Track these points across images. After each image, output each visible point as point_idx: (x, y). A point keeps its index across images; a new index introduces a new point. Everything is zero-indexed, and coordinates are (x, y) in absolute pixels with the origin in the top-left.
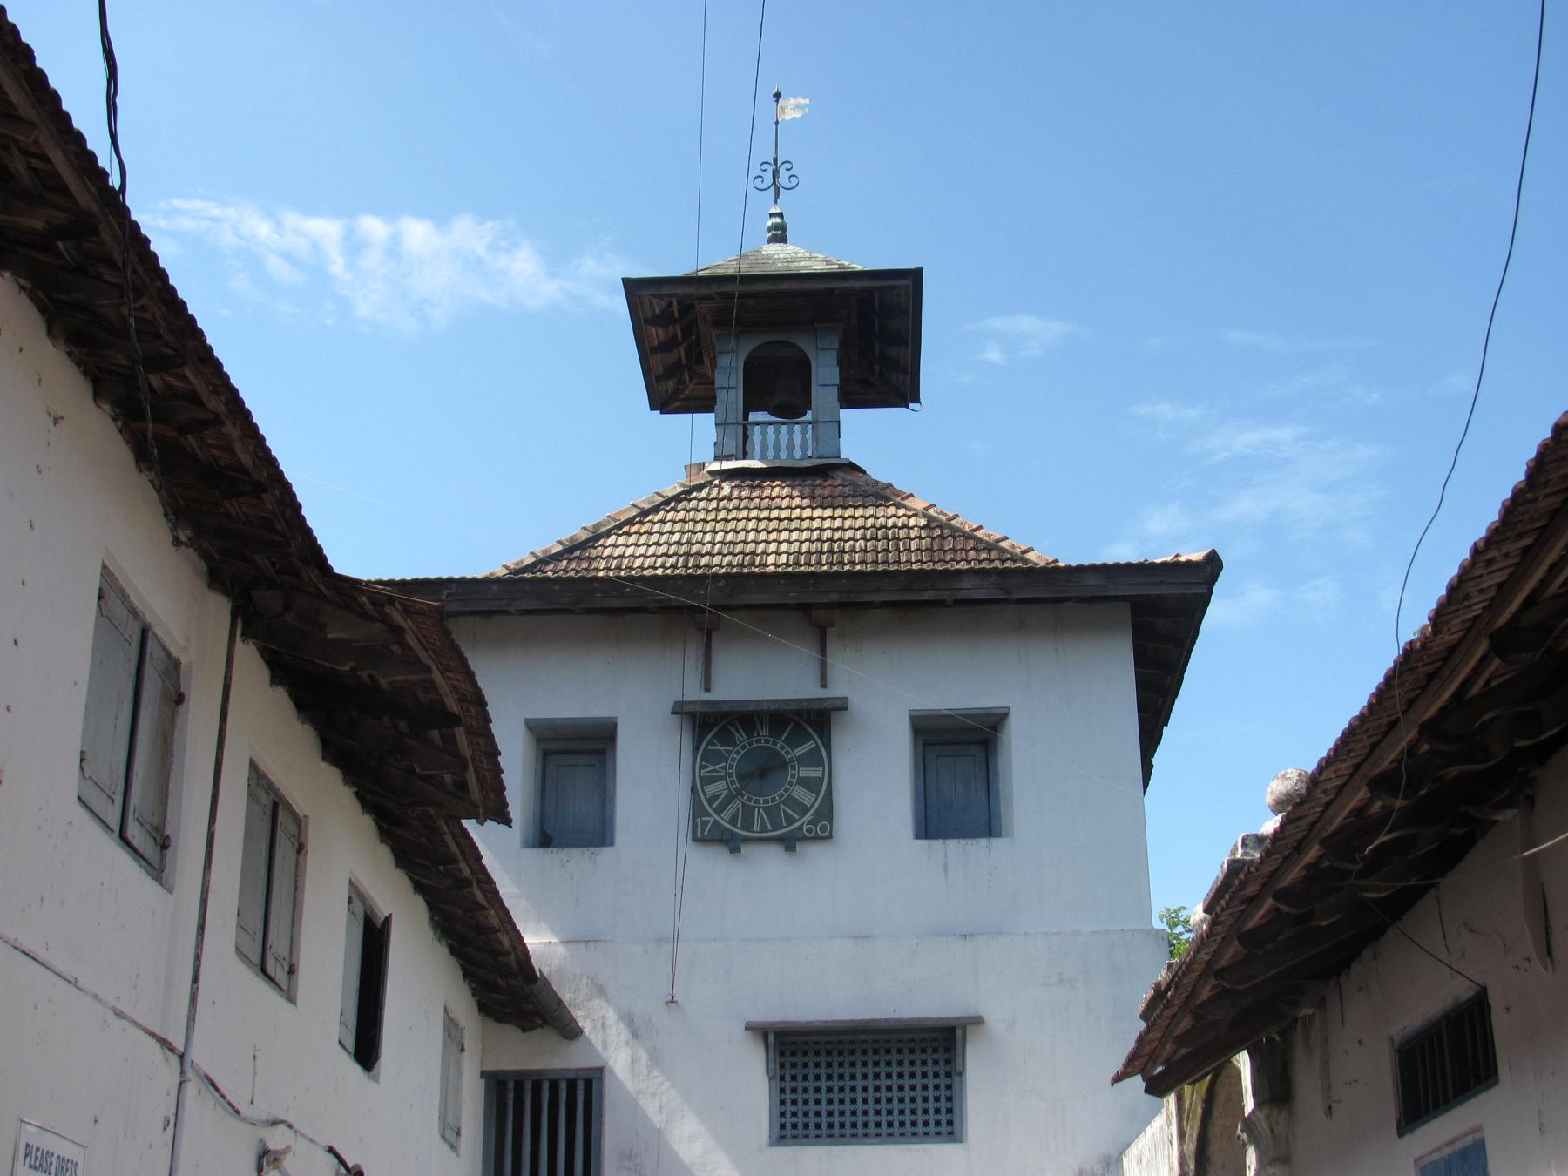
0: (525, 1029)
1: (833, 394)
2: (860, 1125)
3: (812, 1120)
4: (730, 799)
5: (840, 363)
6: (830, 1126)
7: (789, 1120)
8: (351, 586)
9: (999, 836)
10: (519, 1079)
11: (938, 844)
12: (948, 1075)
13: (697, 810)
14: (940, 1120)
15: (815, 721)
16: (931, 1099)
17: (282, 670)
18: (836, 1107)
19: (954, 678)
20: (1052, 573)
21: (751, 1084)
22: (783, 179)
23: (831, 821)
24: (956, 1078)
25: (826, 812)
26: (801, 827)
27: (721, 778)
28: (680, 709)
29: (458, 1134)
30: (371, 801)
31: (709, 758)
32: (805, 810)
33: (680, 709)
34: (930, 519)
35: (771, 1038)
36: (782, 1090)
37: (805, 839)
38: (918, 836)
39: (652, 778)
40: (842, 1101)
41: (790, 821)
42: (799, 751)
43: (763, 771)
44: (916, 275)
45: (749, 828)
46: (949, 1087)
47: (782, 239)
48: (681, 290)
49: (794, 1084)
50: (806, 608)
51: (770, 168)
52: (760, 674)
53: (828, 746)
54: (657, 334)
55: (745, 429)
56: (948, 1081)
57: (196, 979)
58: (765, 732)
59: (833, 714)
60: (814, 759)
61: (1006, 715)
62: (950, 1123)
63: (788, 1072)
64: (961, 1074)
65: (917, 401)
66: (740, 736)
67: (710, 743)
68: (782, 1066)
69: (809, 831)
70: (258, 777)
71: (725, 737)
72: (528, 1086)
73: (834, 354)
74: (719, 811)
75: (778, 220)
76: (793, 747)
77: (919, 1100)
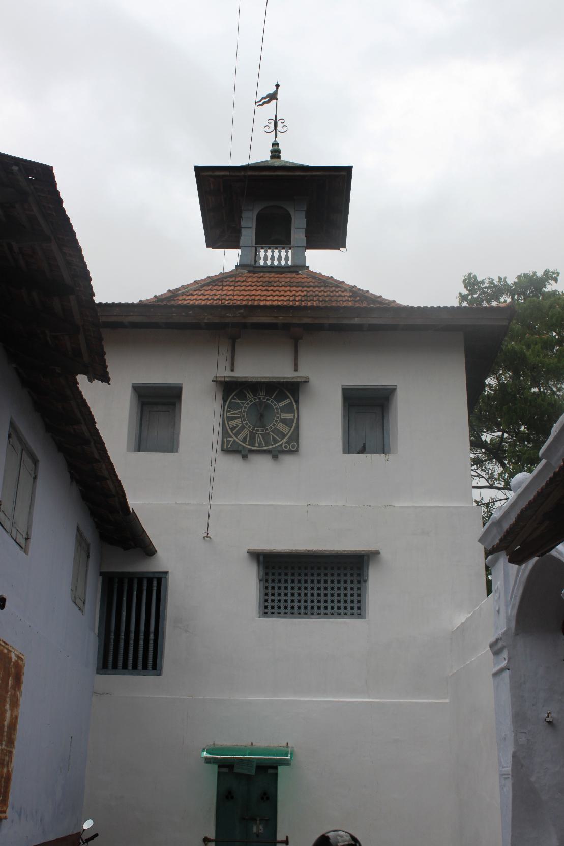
0: (125, 549)
2: (309, 608)
3: (282, 604)
4: (243, 428)
6: (293, 608)
7: (269, 604)
10: (121, 577)
12: (359, 582)
13: (225, 434)
14: (353, 606)
16: (349, 595)
18: (296, 598)
21: (249, 582)
22: (280, 128)
23: (298, 442)
24: (363, 584)
25: (295, 437)
27: (238, 417)
29: (84, 603)
31: (232, 406)
32: (284, 436)
35: (261, 558)
36: (267, 588)
37: (284, 452)
38: (344, 452)
39: (201, 416)
40: (299, 595)
41: (275, 441)
42: (282, 404)
43: (261, 415)
44: (349, 170)
45: (252, 444)
46: (359, 589)
49: (273, 584)
50: (286, 327)
51: (273, 122)
53: (297, 402)
55: (256, 250)
56: (358, 585)
60: (289, 409)
62: (359, 608)
63: (270, 578)
64: (365, 581)
65: (344, 247)
66: (250, 396)
67: (233, 398)
68: (267, 574)
69: (286, 447)
72: (126, 581)
73: (303, 214)
74: (236, 435)
75: (276, 147)
76: (279, 402)
77: (342, 595)
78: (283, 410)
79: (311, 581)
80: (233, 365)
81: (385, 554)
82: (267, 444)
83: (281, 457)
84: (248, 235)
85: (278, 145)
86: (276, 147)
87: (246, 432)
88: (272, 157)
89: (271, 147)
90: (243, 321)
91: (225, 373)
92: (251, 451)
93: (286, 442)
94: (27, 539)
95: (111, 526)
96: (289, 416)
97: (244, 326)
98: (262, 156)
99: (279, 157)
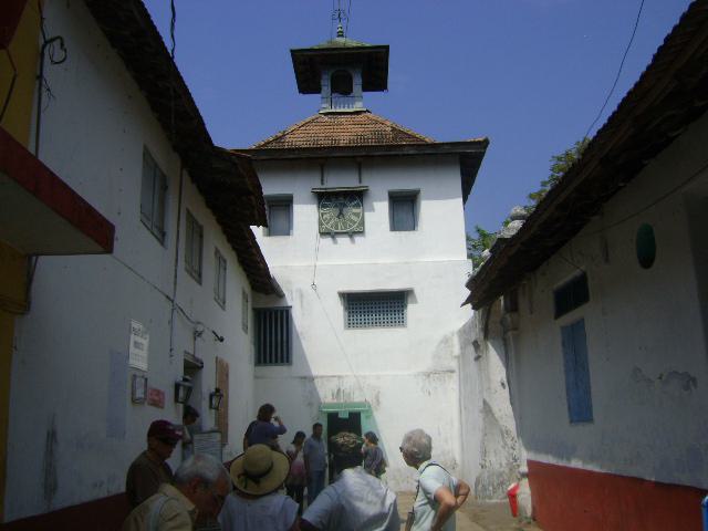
1: (360, 87)
8: (220, 151)
11: (403, 234)
13: (320, 224)
17: (194, 179)
19: (403, 182)
20: (434, 145)
21: (338, 310)
22: (342, 15)
25: (362, 223)
30: (220, 221)
31: (324, 206)
44: (387, 48)
47: (342, 36)
48: (309, 53)
57: (176, 277)
60: (358, 206)
70: (188, 211)
71: (328, 199)
79: (375, 306)
80: (322, 180)
81: (417, 292)
82: (346, 228)
84: (326, 89)
91: (317, 184)
94: (224, 303)
95: (260, 280)
97: (326, 158)
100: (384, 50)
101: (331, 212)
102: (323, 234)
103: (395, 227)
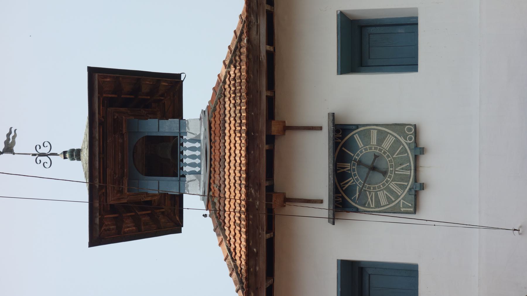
5: (146, 117)
9: (417, 18)
13: (395, 211)
15: (342, 133)
19: (318, 45)
26: (409, 145)
27: (377, 196)
28: (333, 220)
32: (397, 141)
33: (333, 220)
34: (231, 62)
41: (404, 151)
42: (360, 144)
44: (94, 73)
52: (312, 168)
53: (357, 126)
54: (129, 226)
58: (348, 166)
59: (336, 123)
60: (366, 135)
61: (341, 12)
66: (350, 181)
69: (410, 139)
71: (350, 191)
76: (358, 148)
78: (367, 142)
83: (422, 144)
85: (65, 153)
86: (67, 155)
87: (393, 186)
88: (79, 159)
89: (68, 160)
90: (264, 189)
92: (416, 180)
93: (406, 140)
96: (374, 135)
98: (79, 170)
99: (79, 151)
100: (96, 75)
101: (380, 191)
102: (416, 209)
103: (408, 62)
